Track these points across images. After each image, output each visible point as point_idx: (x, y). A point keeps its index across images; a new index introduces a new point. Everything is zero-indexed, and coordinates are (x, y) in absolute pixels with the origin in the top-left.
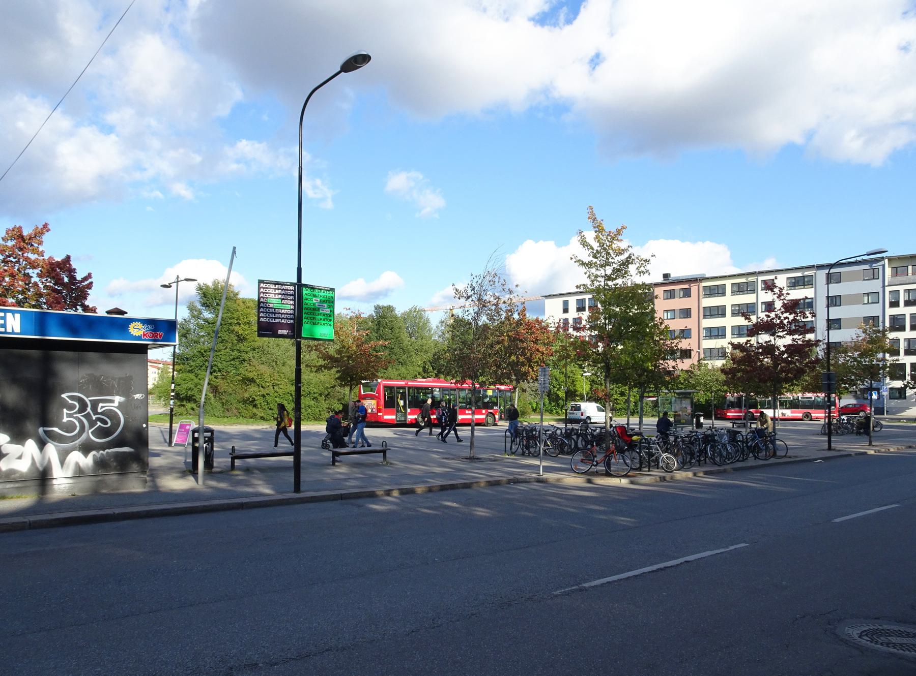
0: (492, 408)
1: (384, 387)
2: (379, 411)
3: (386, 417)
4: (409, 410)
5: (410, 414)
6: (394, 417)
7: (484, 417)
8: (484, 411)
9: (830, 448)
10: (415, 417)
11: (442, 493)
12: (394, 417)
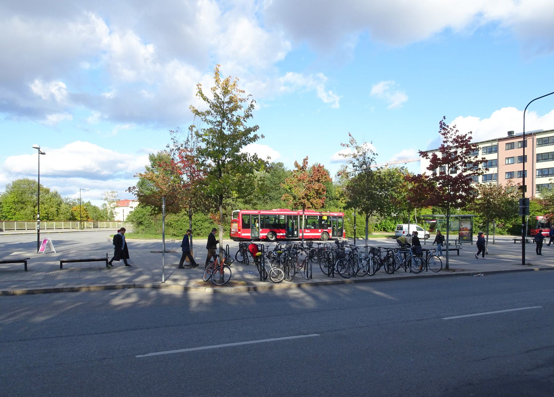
0: (327, 228)
1: (242, 215)
2: (239, 230)
3: (243, 235)
4: (261, 230)
5: (261, 232)
6: (249, 234)
7: (320, 234)
8: (320, 231)
9: (524, 263)
10: (266, 234)
11: (29, 296)
12: (249, 234)
